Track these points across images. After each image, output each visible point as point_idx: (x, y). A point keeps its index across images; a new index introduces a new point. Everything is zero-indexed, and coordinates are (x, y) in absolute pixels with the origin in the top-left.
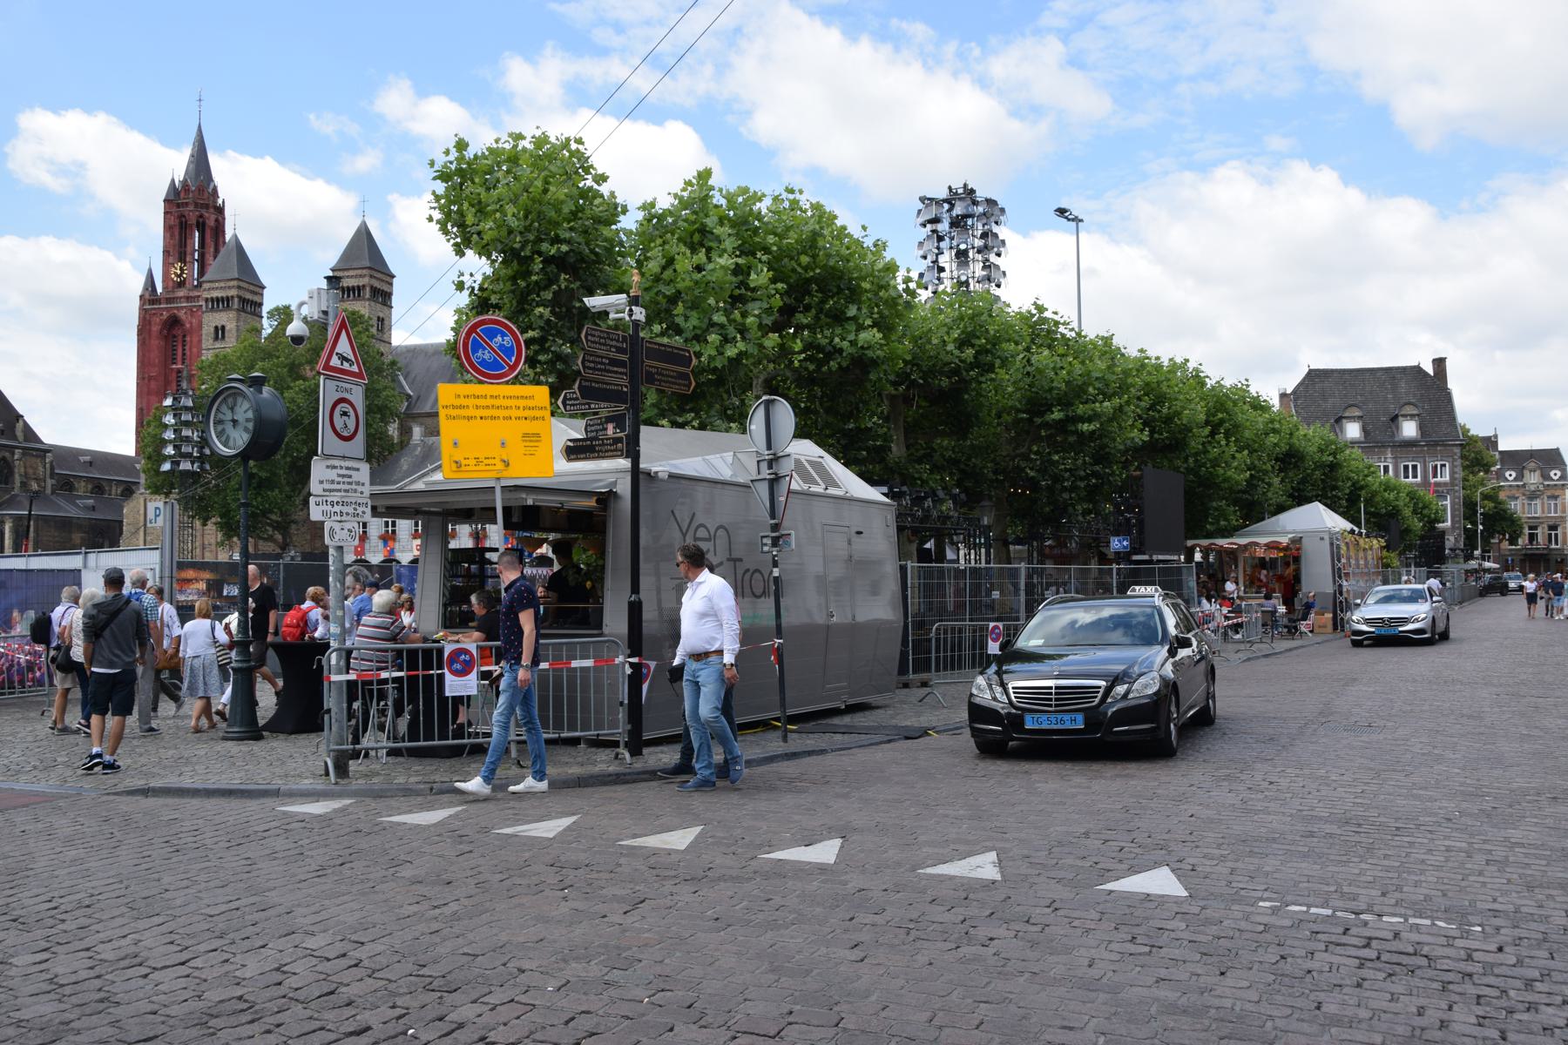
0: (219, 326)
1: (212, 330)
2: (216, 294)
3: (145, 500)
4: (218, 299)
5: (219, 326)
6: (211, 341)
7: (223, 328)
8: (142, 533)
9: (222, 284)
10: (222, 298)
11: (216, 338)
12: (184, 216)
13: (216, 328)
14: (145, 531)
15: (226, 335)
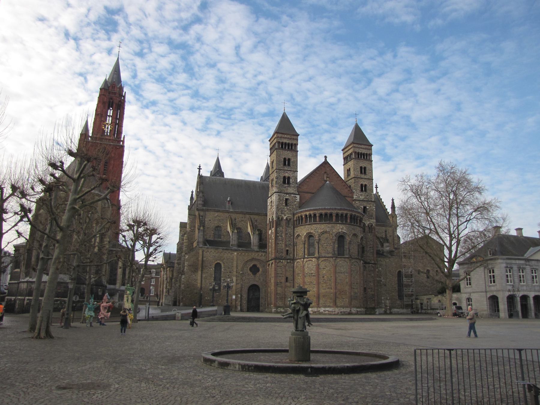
0: (287, 158)
1: (283, 160)
2: (285, 141)
3: (203, 252)
4: (285, 143)
5: (287, 158)
6: (282, 165)
7: (289, 160)
8: (200, 272)
9: (289, 136)
10: (289, 144)
11: (285, 164)
12: (112, 99)
13: (285, 159)
14: (202, 271)
15: (291, 164)
